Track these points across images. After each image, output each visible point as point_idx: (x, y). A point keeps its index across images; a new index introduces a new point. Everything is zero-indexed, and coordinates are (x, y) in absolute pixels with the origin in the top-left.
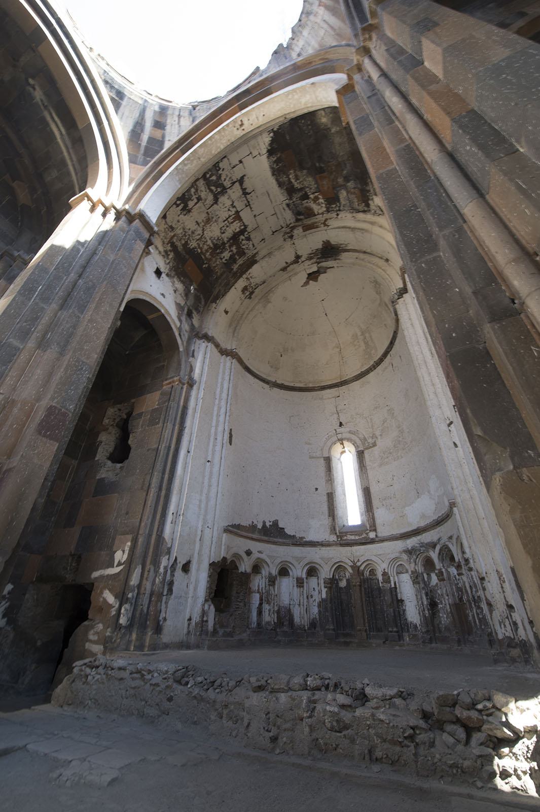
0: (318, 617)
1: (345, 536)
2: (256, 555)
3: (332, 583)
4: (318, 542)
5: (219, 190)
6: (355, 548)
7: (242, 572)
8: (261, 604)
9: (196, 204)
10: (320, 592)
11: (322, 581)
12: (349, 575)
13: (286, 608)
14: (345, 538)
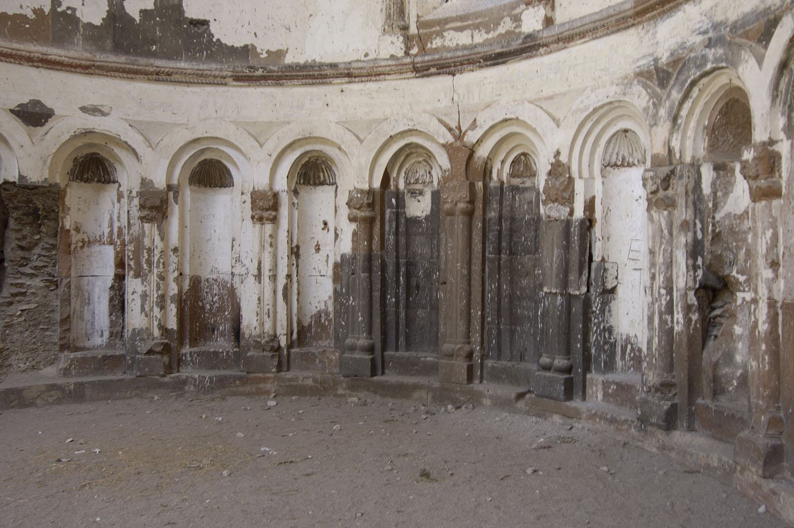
0: (331, 309)
1: (440, 34)
4: (333, 66)
8: (120, 278)
12: (440, 173)
13: (223, 285)
14: (437, 43)
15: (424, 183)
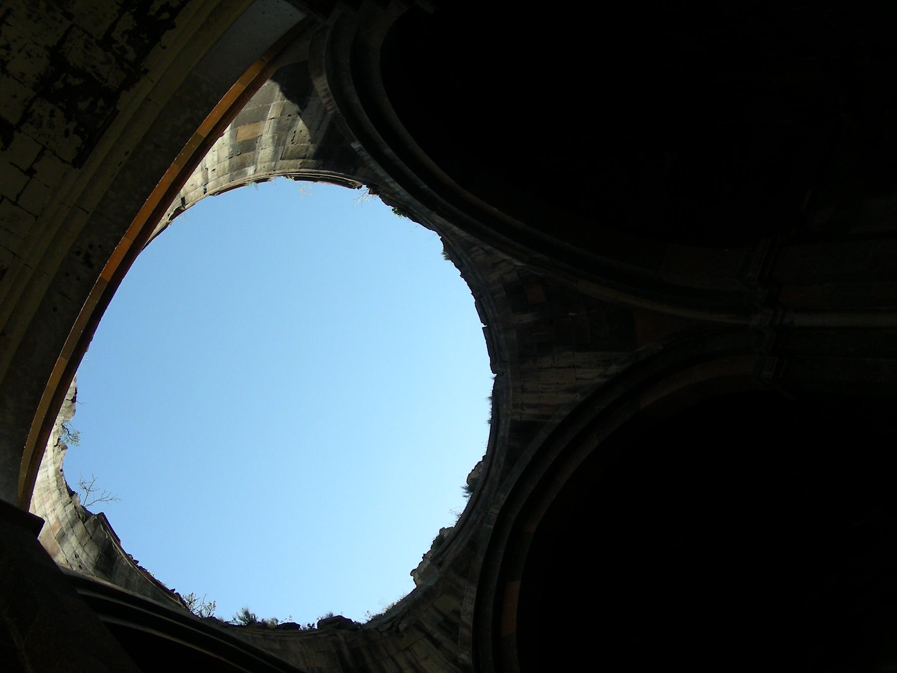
5: (59, 85)
9: (113, 27)
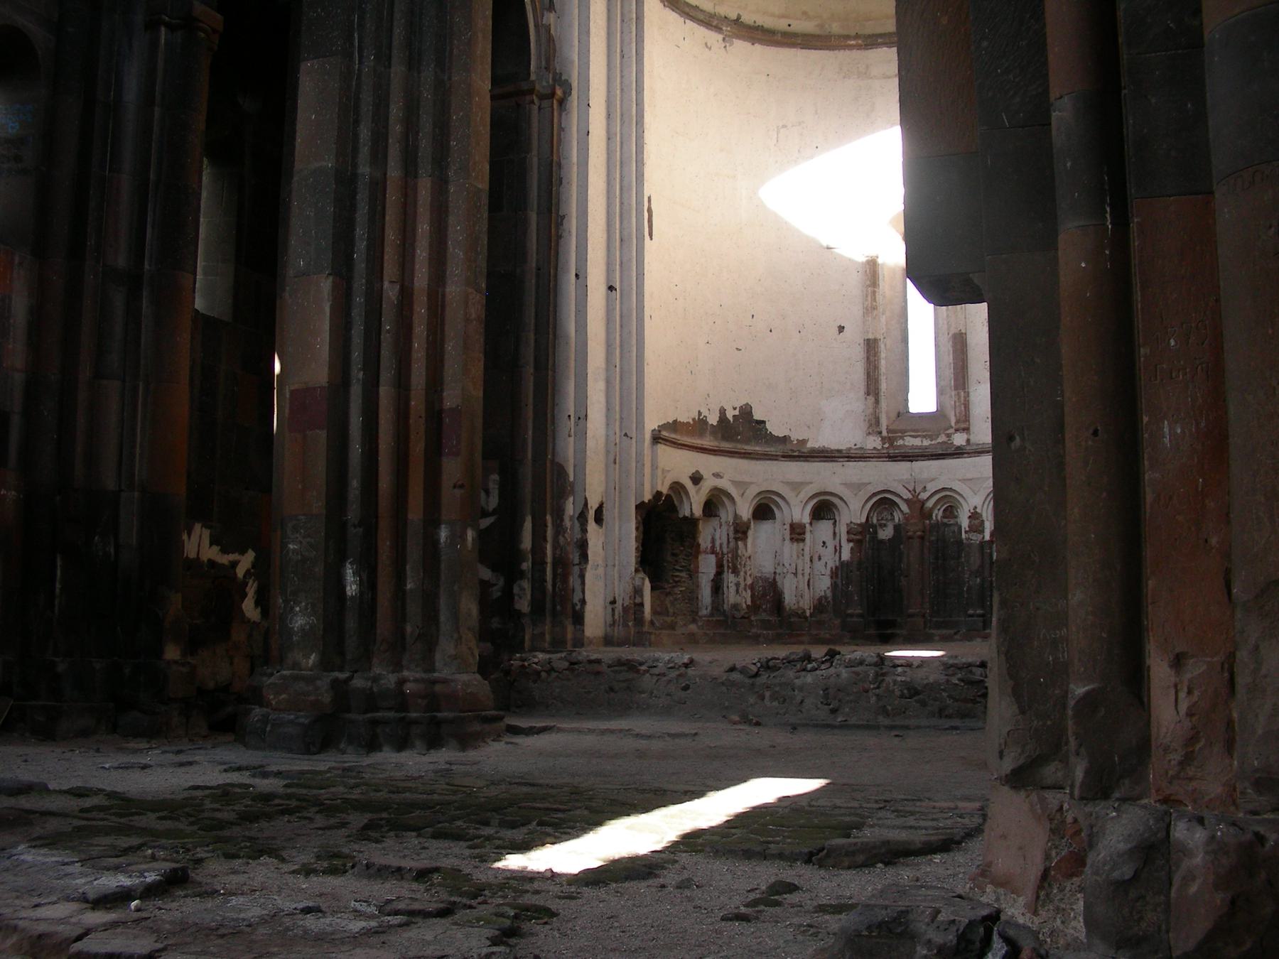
0: (829, 594)
1: (902, 438)
2: (708, 483)
3: (863, 535)
4: (839, 451)
6: (918, 465)
7: (685, 518)
8: (719, 573)
10: (838, 550)
11: (843, 529)
13: (766, 580)
14: (900, 442)
15: (886, 520)
